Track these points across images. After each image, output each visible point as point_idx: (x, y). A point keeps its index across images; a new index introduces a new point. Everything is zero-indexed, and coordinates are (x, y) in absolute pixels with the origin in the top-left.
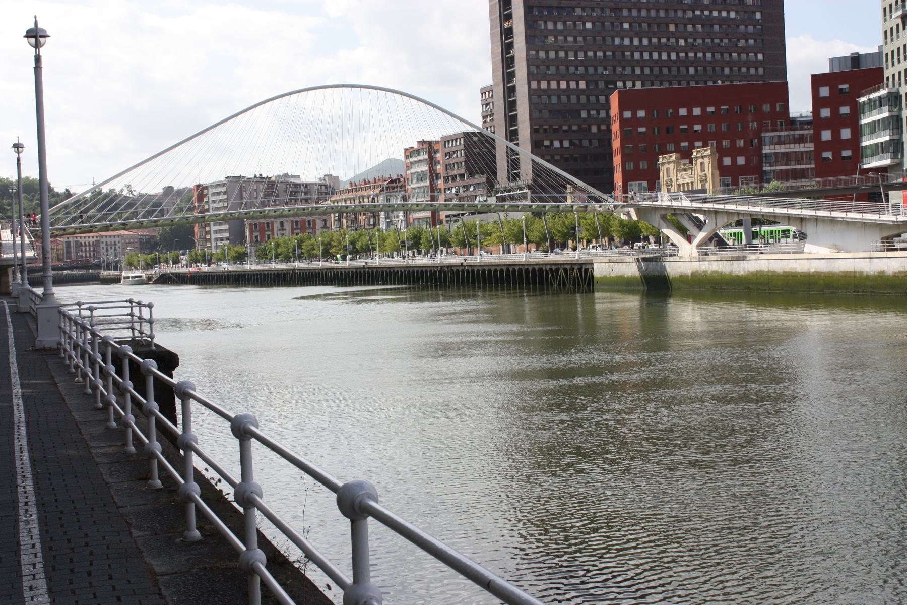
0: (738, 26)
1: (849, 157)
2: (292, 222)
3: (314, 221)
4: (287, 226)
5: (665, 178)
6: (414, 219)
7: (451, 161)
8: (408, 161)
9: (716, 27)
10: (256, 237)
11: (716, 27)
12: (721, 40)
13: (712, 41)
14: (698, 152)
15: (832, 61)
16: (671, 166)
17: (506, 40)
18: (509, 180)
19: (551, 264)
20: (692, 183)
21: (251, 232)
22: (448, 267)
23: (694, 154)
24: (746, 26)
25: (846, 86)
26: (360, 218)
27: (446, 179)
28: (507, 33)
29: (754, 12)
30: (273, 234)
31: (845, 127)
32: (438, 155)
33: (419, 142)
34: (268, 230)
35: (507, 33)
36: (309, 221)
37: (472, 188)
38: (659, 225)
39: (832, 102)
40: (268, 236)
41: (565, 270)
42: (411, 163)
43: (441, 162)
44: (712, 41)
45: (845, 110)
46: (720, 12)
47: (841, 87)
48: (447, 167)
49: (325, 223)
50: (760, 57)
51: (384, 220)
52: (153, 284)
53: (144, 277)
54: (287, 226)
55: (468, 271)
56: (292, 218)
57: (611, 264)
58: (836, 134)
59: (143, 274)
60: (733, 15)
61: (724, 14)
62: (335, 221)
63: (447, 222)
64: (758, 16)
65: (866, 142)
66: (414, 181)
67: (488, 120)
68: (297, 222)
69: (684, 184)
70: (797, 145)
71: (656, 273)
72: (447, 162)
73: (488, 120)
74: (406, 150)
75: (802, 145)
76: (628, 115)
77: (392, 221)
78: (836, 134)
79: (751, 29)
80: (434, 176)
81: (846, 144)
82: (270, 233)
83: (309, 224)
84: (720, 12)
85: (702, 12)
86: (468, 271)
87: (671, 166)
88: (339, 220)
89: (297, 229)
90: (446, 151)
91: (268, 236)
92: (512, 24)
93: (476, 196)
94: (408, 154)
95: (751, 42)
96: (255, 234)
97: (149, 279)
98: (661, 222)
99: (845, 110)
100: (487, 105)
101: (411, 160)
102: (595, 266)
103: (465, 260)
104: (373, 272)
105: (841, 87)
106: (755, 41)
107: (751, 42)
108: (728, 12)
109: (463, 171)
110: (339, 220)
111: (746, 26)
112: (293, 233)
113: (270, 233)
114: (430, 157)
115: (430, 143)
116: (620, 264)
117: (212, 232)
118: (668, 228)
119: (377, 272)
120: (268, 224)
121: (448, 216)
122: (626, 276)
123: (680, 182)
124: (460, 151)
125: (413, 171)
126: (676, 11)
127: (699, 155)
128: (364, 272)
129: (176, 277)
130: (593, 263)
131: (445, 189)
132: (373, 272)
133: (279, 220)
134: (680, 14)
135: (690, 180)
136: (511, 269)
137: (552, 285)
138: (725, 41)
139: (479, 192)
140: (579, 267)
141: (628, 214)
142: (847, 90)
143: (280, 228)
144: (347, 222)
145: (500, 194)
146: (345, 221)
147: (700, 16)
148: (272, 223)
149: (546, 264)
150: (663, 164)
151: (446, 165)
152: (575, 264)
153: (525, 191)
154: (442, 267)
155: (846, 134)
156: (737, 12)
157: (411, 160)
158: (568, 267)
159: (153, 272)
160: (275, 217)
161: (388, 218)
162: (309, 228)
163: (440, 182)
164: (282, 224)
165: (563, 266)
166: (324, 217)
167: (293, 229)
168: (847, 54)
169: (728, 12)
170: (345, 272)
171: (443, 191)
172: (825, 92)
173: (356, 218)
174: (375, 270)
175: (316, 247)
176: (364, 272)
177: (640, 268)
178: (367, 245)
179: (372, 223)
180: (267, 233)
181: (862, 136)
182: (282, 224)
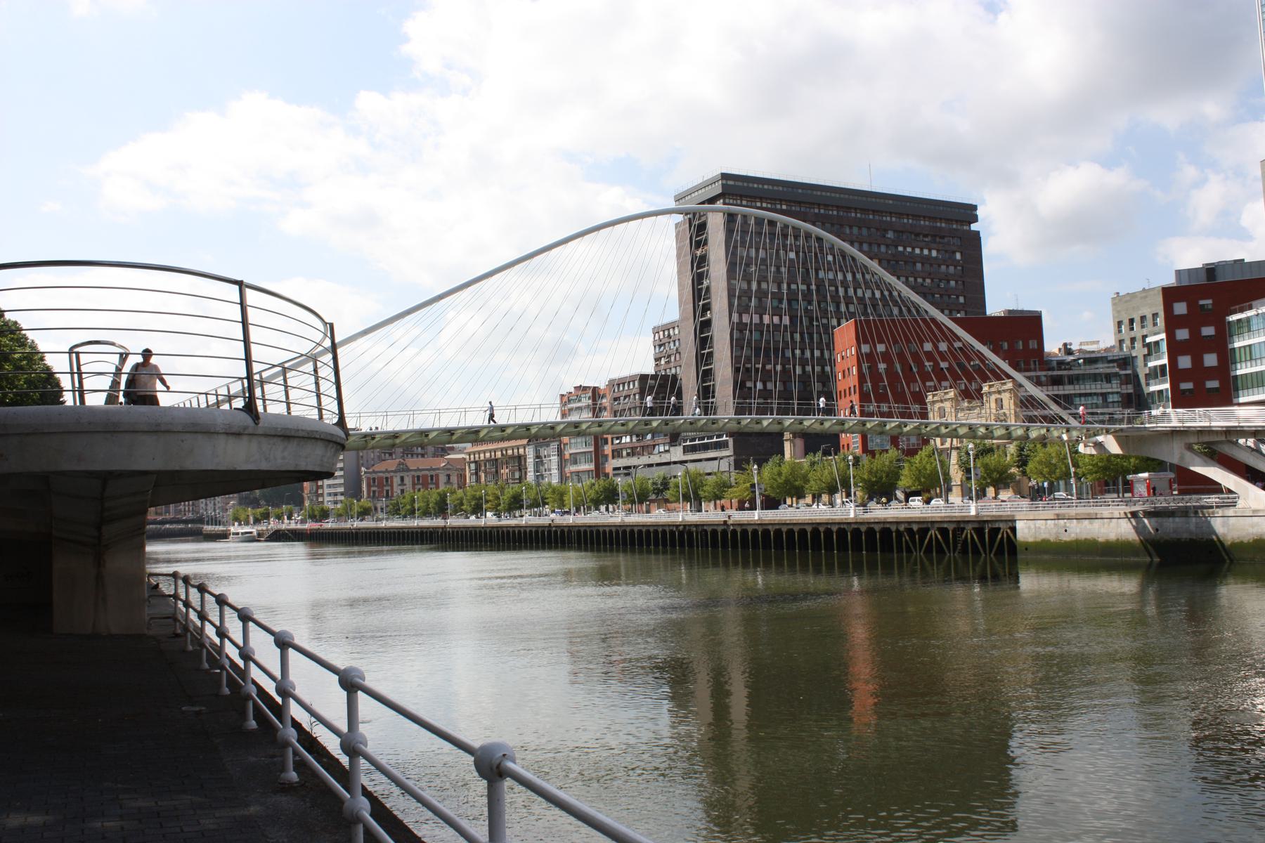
0: (939, 266)
1: (1216, 389)
2: (413, 477)
3: (437, 476)
4: (408, 481)
6: (571, 473)
9: (919, 266)
10: (374, 492)
11: (919, 266)
12: (924, 280)
13: (916, 279)
14: (990, 386)
15: (1178, 273)
16: (947, 405)
17: (697, 269)
19: (909, 523)
21: (369, 486)
22: (696, 526)
23: (930, 398)
24: (948, 266)
25: (1209, 302)
26: (502, 471)
28: (699, 263)
29: (954, 252)
30: (392, 489)
31: (1210, 351)
33: (575, 388)
34: (387, 485)
35: (699, 263)
36: (432, 476)
37: (649, 437)
38: (1182, 458)
39: (1194, 320)
40: (387, 491)
41: (944, 531)
42: (571, 410)
43: (608, 408)
44: (916, 279)
45: (1208, 331)
46: (922, 249)
47: (1202, 302)
49: (449, 479)
50: (962, 300)
51: (532, 474)
52: (266, 541)
53: (255, 534)
54: (408, 481)
55: (734, 532)
56: (413, 473)
57: (1062, 522)
58: (1197, 361)
59: (254, 530)
60: (934, 253)
61: (926, 252)
62: (471, 474)
64: (958, 256)
65: (1242, 370)
67: (663, 362)
68: (418, 477)
70: (1055, 387)
71: (1185, 536)
73: (663, 362)
74: (562, 396)
75: (1061, 387)
76: (865, 348)
77: (542, 475)
78: (1197, 361)
79: (951, 269)
81: (1211, 373)
82: (388, 488)
83: (432, 479)
84: (922, 249)
85: (905, 248)
86: (734, 532)
87: (947, 405)
88: (476, 474)
89: (418, 484)
90: (616, 395)
91: (387, 491)
92: (706, 251)
93: (654, 446)
94: (565, 399)
95: (953, 283)
96: (373, 489)
97: (260, 535)
98: (1188, 455)
99: (1208, 331)
100: (660, 346)
101: (570, 406)
102: (1019, 525)
103: (729, 517)
104: (563, 532)
105: (1202, 302)
106: (957, 282)
107: (953, 283)
108: (930, 251)
110: (476, 474)
111: (948, 266)
112: (414, 488)
113: (388, 488)
115: (595, 390)
116: (1087, 522)
117: (325, 486)
118: (1207, 465)
119: (569, 532)
120: (387, 478)
121: (615, 469)
122: (1100, 540)
124: (634, 395)
126: (879, 245)
127: (993, 389)
128: (549, 532)
129: (292, 533)
130: (1015, 521)
131: (612, 438)
132: (563, 532)
133: (399, 475)
134: (883, 249)
136: (822, 529)
137: (909, 551)
138: (928, 281)
139: (660, 439)
140: (976, 526)
141: (1099, 446)
142: (1210, 307)
143: (399, 482)
144: (485, 476)
145: (688, 443)
147: (902, 253)
148: (392, 477)
149: (898, 523)
150: (934, 402)
152: (968, 522)
153: (724, 438)
154: (685, 526)
155: (1211, 360)
156: (938, 251)
157: (570, 406)
158: (951, 527)
159: (264, 528)
160: (395, 472)
161: (538, 472)
162: (432, 483)
164: (402, 479)
165: (937, 526)
166: (448, 472)
167: (414, 484)
168: (1198, 264)
169: (930, 251)
170: (519, 532)
172: (1180, 308)
173: (497, 472)
174: (566, 530)
175: (465, 501)
176: (549, 532)
177: (1139, 529)
178: (535, 500)
179: (517, 475)
180: (386, 488)
181: (1235, 363)
182: (402, 479)
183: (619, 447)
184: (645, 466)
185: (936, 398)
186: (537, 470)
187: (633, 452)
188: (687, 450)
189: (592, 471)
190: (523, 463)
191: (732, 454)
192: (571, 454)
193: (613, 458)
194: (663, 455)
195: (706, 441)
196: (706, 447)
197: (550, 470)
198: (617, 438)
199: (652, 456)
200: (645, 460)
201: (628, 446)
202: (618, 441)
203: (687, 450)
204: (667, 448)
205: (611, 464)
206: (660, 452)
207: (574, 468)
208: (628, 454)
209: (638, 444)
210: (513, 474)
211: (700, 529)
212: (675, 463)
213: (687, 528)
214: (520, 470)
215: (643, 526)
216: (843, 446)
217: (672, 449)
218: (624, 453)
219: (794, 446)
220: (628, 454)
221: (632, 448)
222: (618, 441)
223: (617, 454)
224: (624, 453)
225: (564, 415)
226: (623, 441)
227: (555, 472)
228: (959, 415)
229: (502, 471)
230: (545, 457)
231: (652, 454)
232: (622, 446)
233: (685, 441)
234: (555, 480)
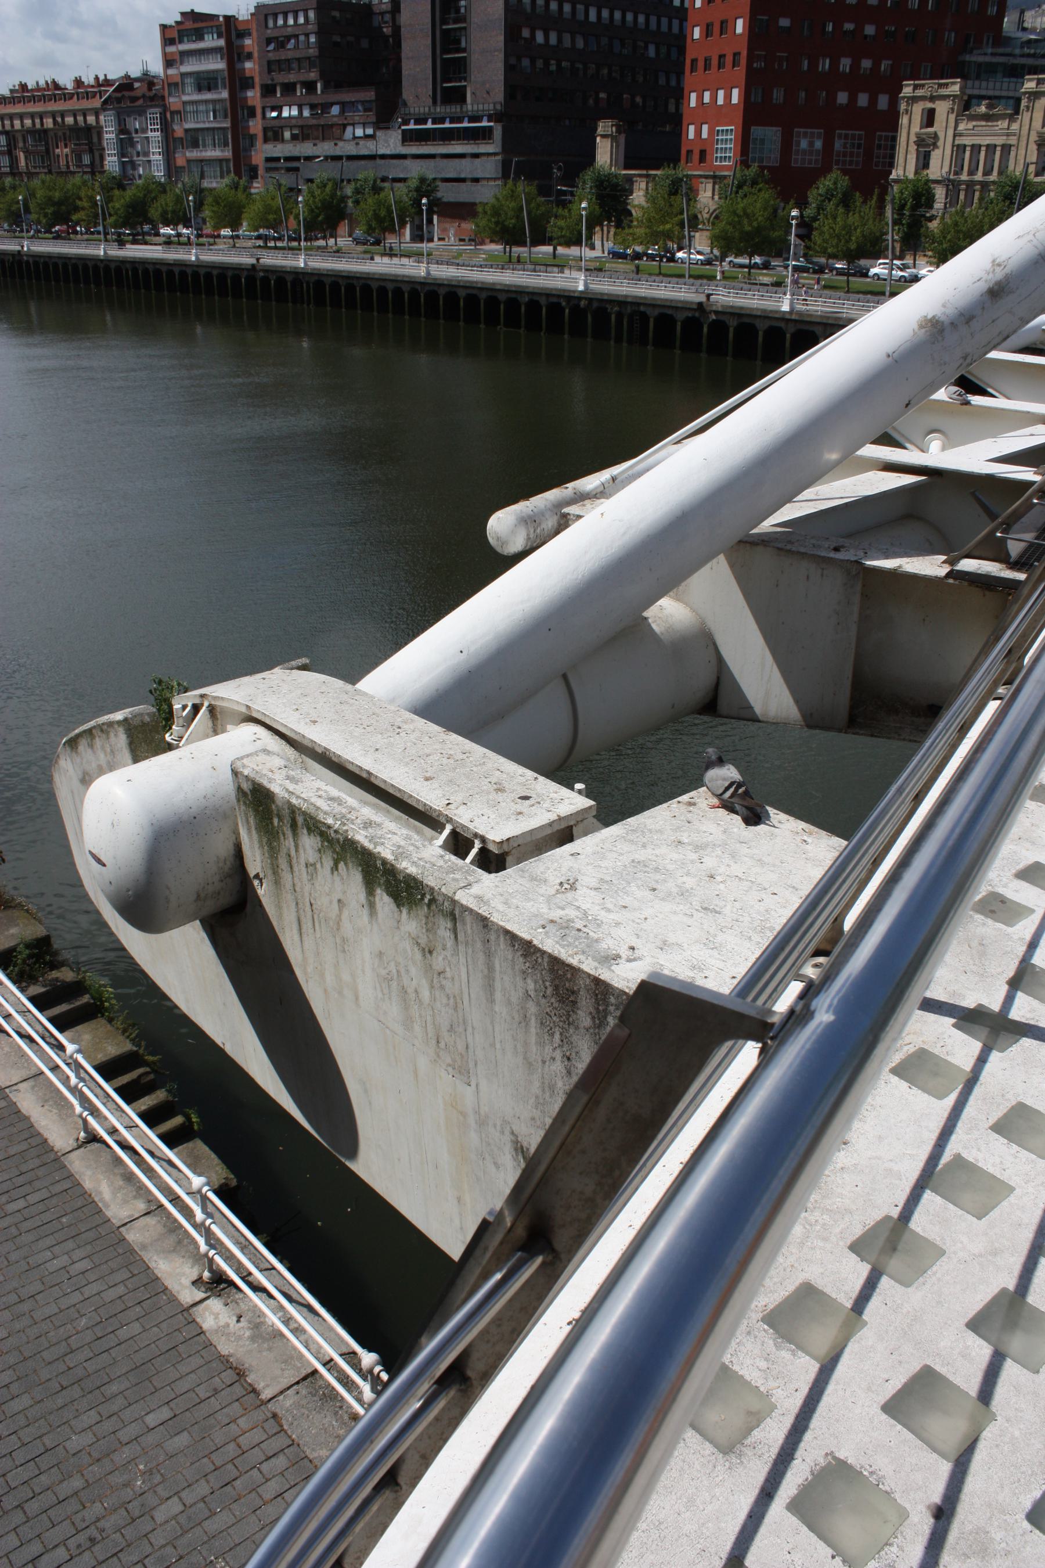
5: (916, 128)
6: (189, 161)
7: (282, 55)
8: (171, 49)
18: (435, 102)
20: (1006, 149)
27: (268, 90)
32: (248, 42)
37: (335, 110)
42: (184, 54)
43: (256, 55)
48: (271, 66)
63: (268, 170)
66: (189, 89)
69: (976, 148)
72: (272, 56)
80: (238, 82)
109: (313, 75)
114: (229, 43)
121: (269, 160)
123: (959, 141)
124: (307, 35)
125: (184, 69)
131: (264, 109)
135: (1000, 141)
139: (358, 115)
145: (412, 126)
146: (22, 156)
151: (269, 63)
153: (485, 123)
154: (590, 300)
161: (123, 155)
163: (253, 96)
171: (259, 111)
183: (276, 123)
184: (326, 158)
185: (920, 93)
186: (122, 154)
187: (304, 132)
188: (408, 137)
189: (227, 160)
190: (95, 140)
191: (498, 150)
192: (187, 131)
193: (266, 140)
194: (362, 142)
195: (447, 125)
196: (447, 136)
197: (147, 154)
198: (273, 109)
199: (341, 144)
200: (326, 148)
201: (294, 122)
202: (274, 114)
203: (408, 137)
204: (370, 131)
205: (262, 152)
206: (355, 138)
207: (193, 154)
208: (294, 137)
209: (314, 122)
210: (79, 158)
211: (629, 309)
212: (383, 157)
213: (595, 305)
214: (91, 151)
215: (481, 289)
216: (689, 152)
217: (379, 134)
218: (287, 135)
219: (617, 147)
220: (294, 137)
221: (302, 127)
222: (274, 114)
223: (273, 134)
224: (287, 135)
225: (169, 63)
226: (285, 113)
227: (156, 157)
228: (962, 127)
229: (58, 151)
230: (136, 131)
231: (341, 139)
232: (282, 123)
233: (406, 122)
234: (159, 173)
